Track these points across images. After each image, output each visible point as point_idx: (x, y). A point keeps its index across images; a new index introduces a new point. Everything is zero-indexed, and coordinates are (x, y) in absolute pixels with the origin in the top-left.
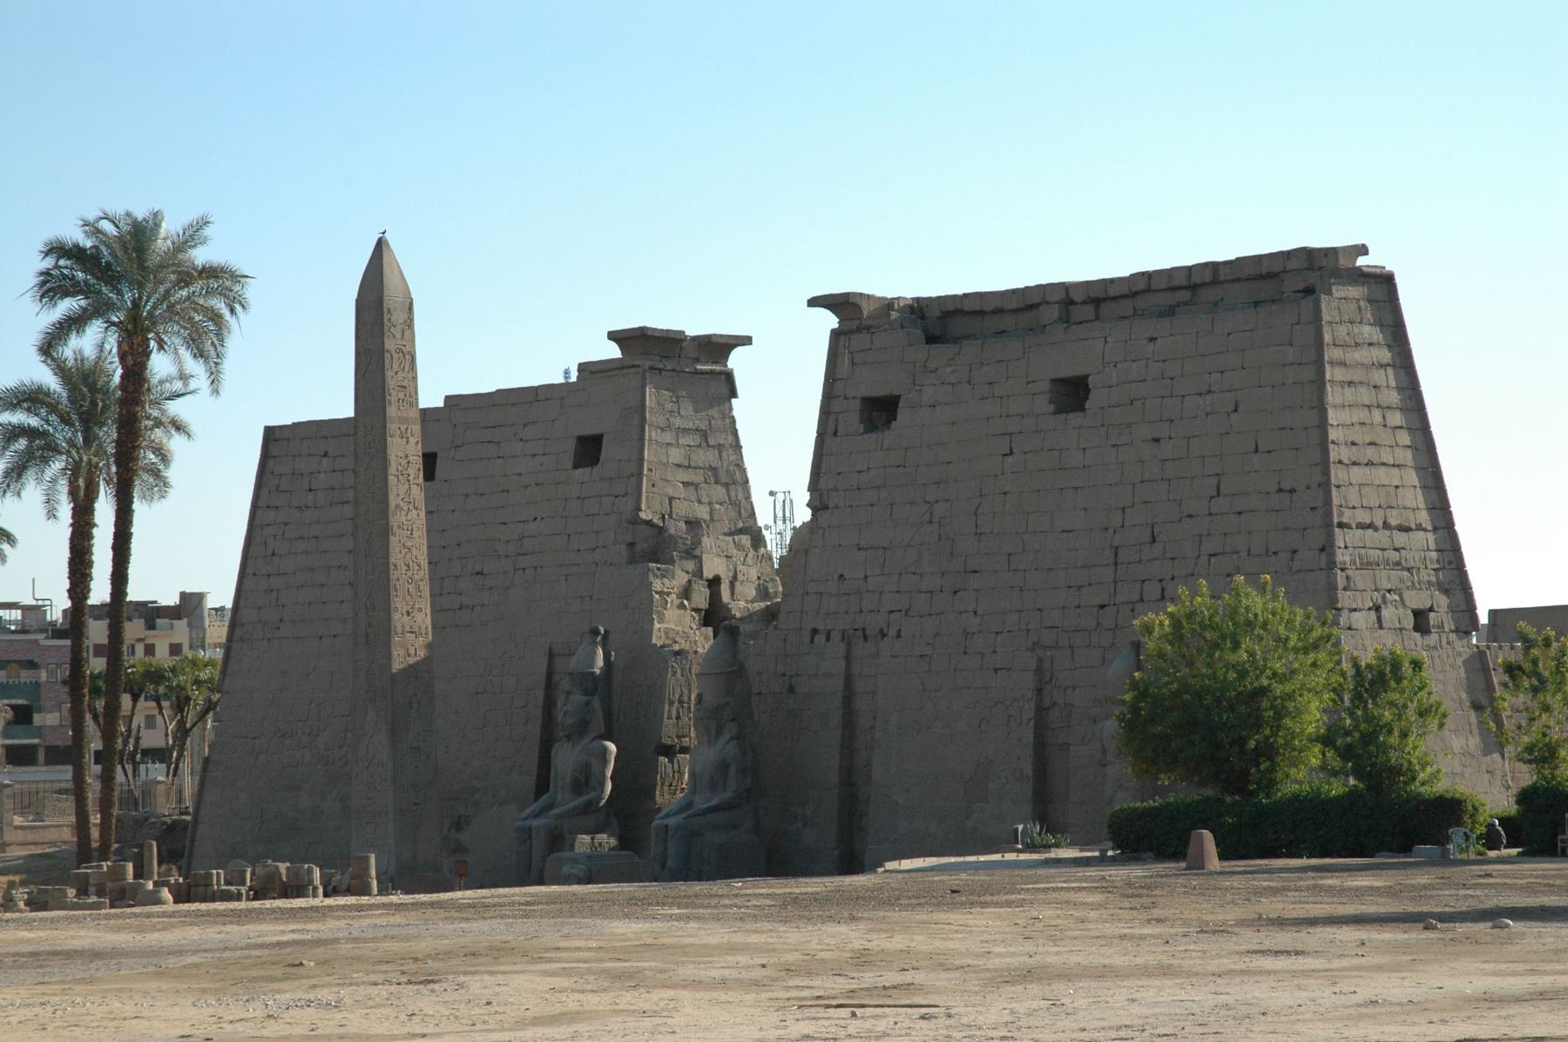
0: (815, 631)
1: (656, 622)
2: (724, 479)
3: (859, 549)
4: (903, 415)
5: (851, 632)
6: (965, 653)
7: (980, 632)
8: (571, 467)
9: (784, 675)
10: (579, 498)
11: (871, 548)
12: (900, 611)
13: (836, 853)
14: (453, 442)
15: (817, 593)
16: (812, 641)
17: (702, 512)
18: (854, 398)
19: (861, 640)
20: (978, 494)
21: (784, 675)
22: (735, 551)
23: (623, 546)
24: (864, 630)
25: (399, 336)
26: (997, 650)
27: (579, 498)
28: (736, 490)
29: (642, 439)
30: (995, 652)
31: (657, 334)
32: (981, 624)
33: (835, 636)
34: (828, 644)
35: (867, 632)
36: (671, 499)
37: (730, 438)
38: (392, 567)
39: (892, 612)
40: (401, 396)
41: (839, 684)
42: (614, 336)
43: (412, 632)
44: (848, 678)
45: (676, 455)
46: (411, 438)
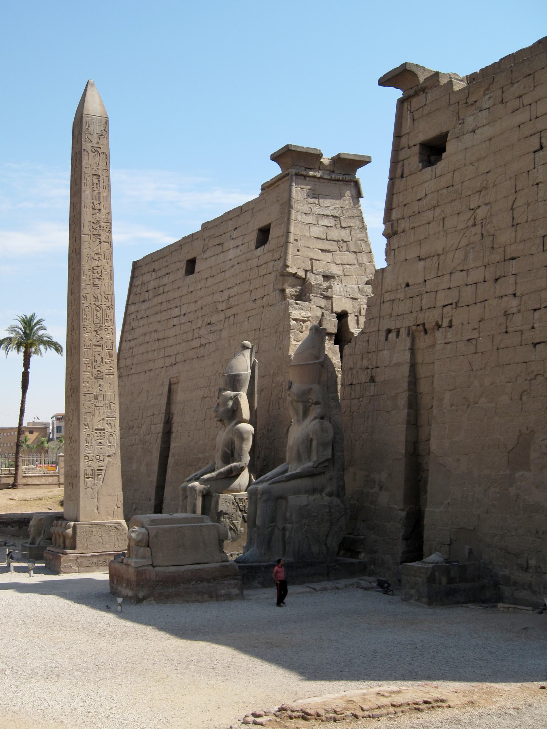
0: (389, 331)
1: (292, 340)
2: (352, 248)
3: (420, 260)
4: (450, 147)
5: (414, 328)
6: (506, 332)
7: (519, 311)
8: (254, 247)
9: (367, 369)
10: (257, 267)
11: (428, 257)
12: (452, 304)
13: (404, 514)
14: (203, 249)
15: (390, 301)
16: (387, 339)
17: (335, 270)
18: (415, 145)
19: (422, 333)
20: (513, 191)
21: (367, 369)
22: (359, 295)
23: (277, 292)
24: (424, 324)
25: (95, 141)
26: (535, 325)
27: (257, 267)
28: (362, 257)
29: (289, 219)
30: (533, 328)
31: (299, 150)
32: (520, 305)
33: (403, 332)
34: (398, 340)
35: (427, 326)
36: (311, 260)
37: (358, 223)
38: (82, 298)
39: (444, 306)
40: (96, 181)
41: (406, 370)
42: (276, 158)
43: (100, 346)
44: (413, 366)
45: (316, 231)
46: (103, 210)
